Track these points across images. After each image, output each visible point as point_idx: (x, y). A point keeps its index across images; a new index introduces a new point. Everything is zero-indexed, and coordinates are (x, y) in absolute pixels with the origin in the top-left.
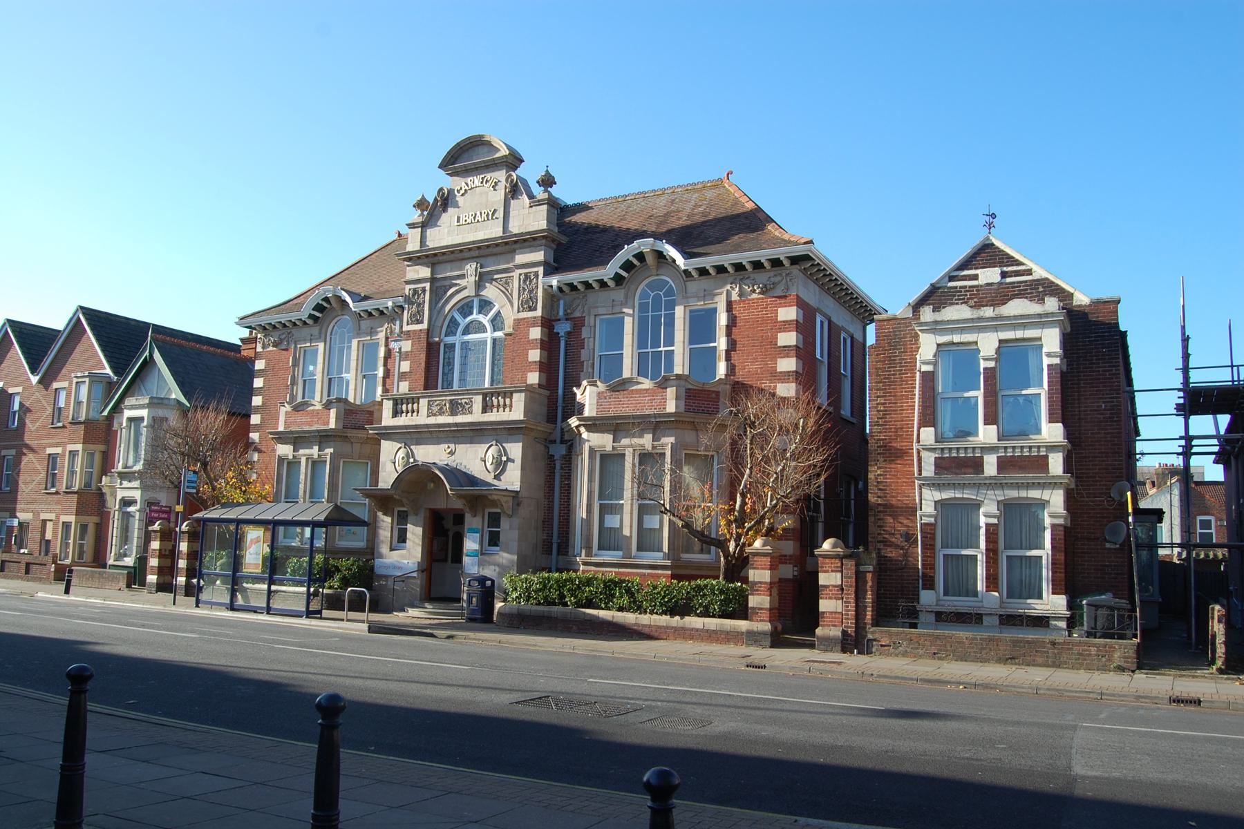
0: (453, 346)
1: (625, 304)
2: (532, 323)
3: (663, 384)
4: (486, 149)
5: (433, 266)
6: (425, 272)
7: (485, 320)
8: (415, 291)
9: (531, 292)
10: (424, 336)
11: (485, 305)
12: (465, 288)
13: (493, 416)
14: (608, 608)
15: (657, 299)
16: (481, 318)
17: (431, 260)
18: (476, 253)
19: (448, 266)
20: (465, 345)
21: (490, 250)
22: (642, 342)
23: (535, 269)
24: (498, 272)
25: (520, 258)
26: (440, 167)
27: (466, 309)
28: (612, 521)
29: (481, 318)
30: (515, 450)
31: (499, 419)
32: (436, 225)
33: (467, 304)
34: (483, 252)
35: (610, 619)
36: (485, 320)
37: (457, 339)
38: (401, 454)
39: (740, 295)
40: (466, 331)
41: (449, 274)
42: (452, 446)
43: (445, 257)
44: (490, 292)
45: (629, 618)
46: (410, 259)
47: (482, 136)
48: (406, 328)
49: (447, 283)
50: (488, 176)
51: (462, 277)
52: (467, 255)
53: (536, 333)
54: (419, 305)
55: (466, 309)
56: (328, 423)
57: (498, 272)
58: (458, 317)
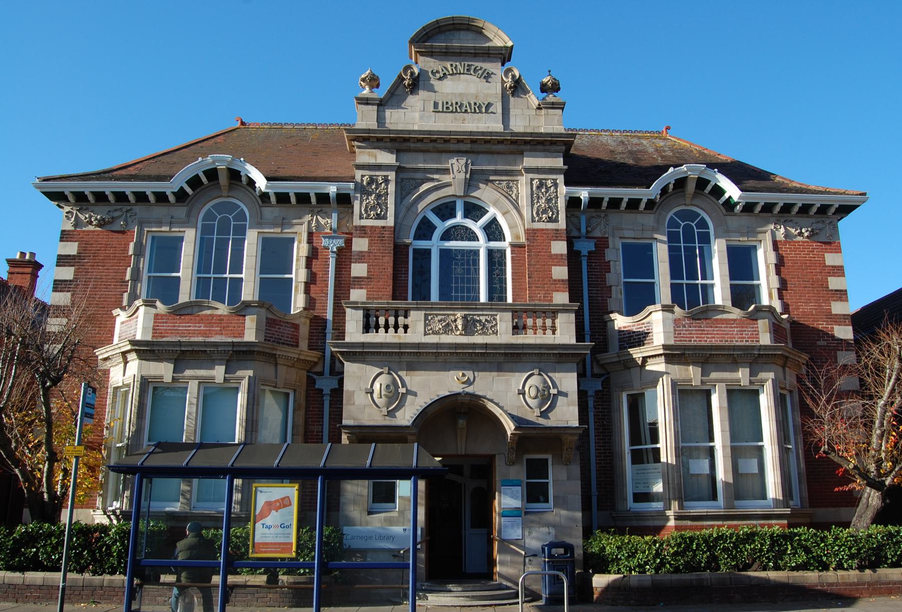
0: (428, 252)
1: (656, 230)
2: (555, 235)
3: (753, 318)
4: (470, 35)
5: (398, 152)
6: (388, 158)
7: (476, 227)
8: (372, 180)
9: (548, 201)
10: (387, 234)
11: (474, 211)
12: (448, 185)
13: (528, 338)
14: (777, 568)
15: (688, 230)
16: (469, 223)
17: (397, 145)
18: (468, 147)
19: (420, 156)
20: (446, 254)
21: (488, 146)
22: (675, 272)
23: (554, 177)
24: (496, 173)
25: (529, 161)
26: (413, 41)
27: (445, 210)
28: (701, 466)
29: (469, 223)
30: (568, 381)
31: (539, 341)
32: (399, 106)
33: (446, 205)
34: (476, 147)
35: (785, 580)
36: (476, 227)
37: (435, 245)
38: (384, 380)
39: (786, 236)
40: (447, 235)
41: (421, 165)
42: (469, 374)
43: (419, 145)
44: (485, 194)
45: (811, 577)
46: (364, 140)
47: (473, 20)
48: (357, 222)
49: (419, 176)
50: (479, 64)
51: (446, 171)
52: (452, 147)
53: (560, 247)
54: (379, 196)
55: (445, 210)
56: (242, 334)
57: (496, 173)
58: (434, 219)
